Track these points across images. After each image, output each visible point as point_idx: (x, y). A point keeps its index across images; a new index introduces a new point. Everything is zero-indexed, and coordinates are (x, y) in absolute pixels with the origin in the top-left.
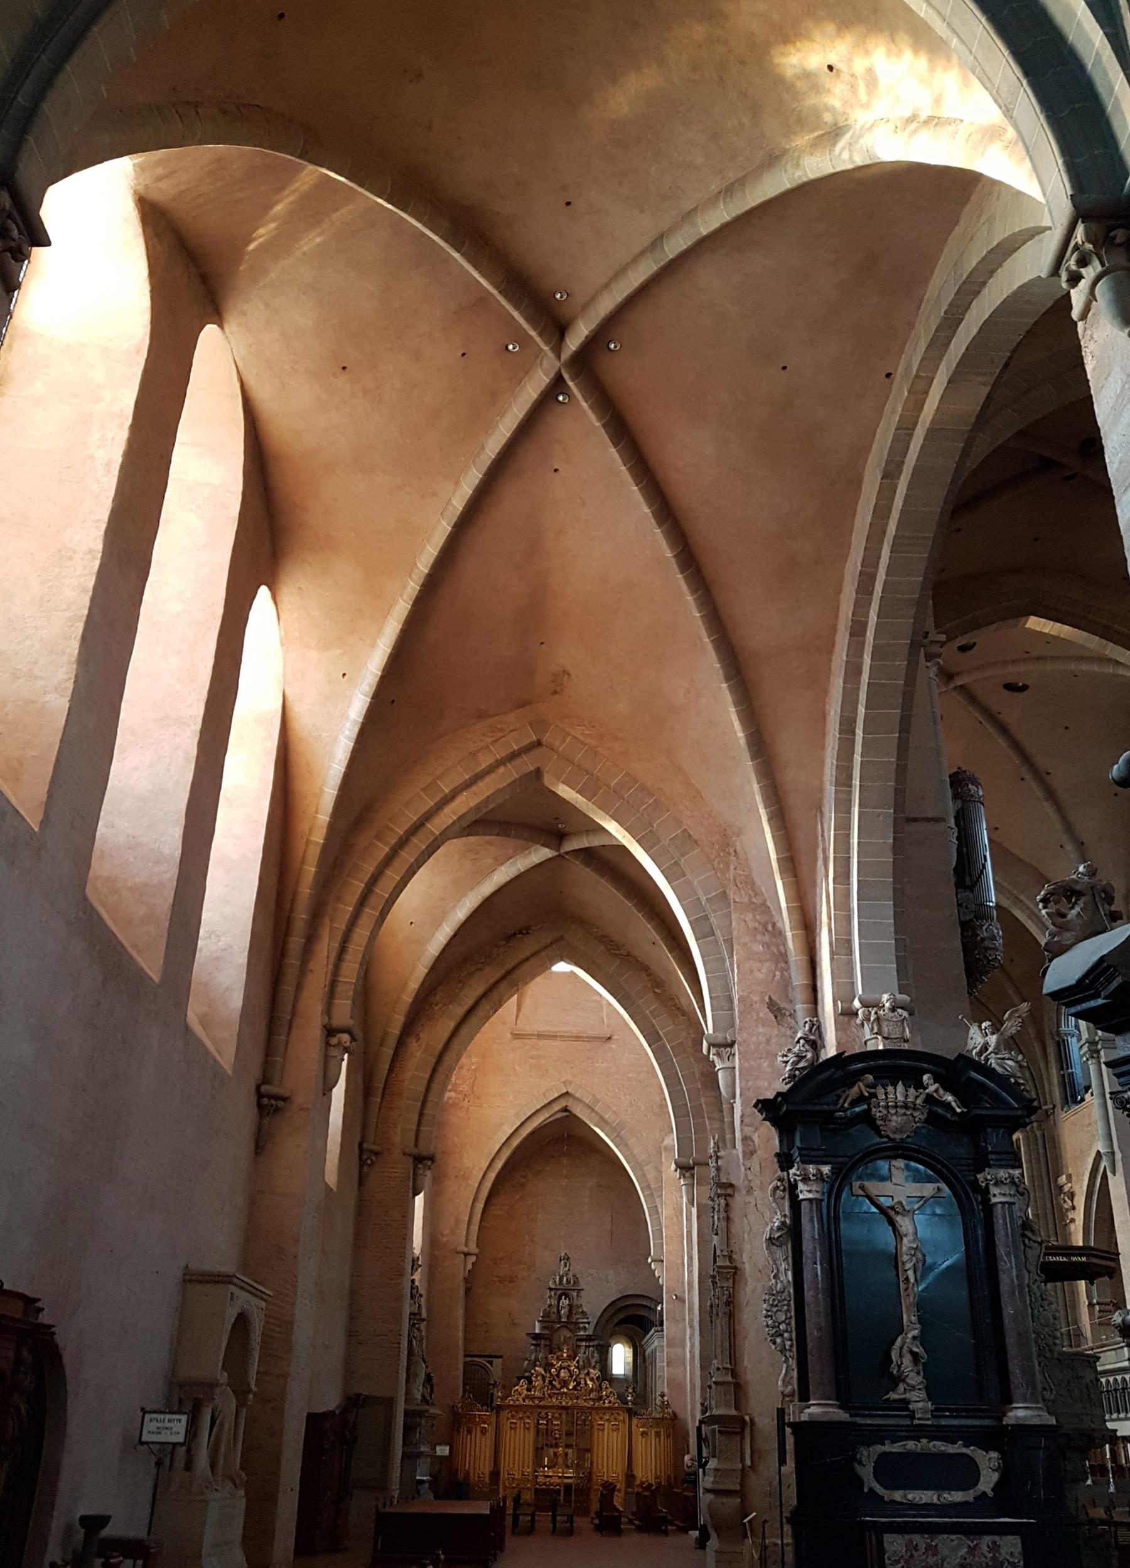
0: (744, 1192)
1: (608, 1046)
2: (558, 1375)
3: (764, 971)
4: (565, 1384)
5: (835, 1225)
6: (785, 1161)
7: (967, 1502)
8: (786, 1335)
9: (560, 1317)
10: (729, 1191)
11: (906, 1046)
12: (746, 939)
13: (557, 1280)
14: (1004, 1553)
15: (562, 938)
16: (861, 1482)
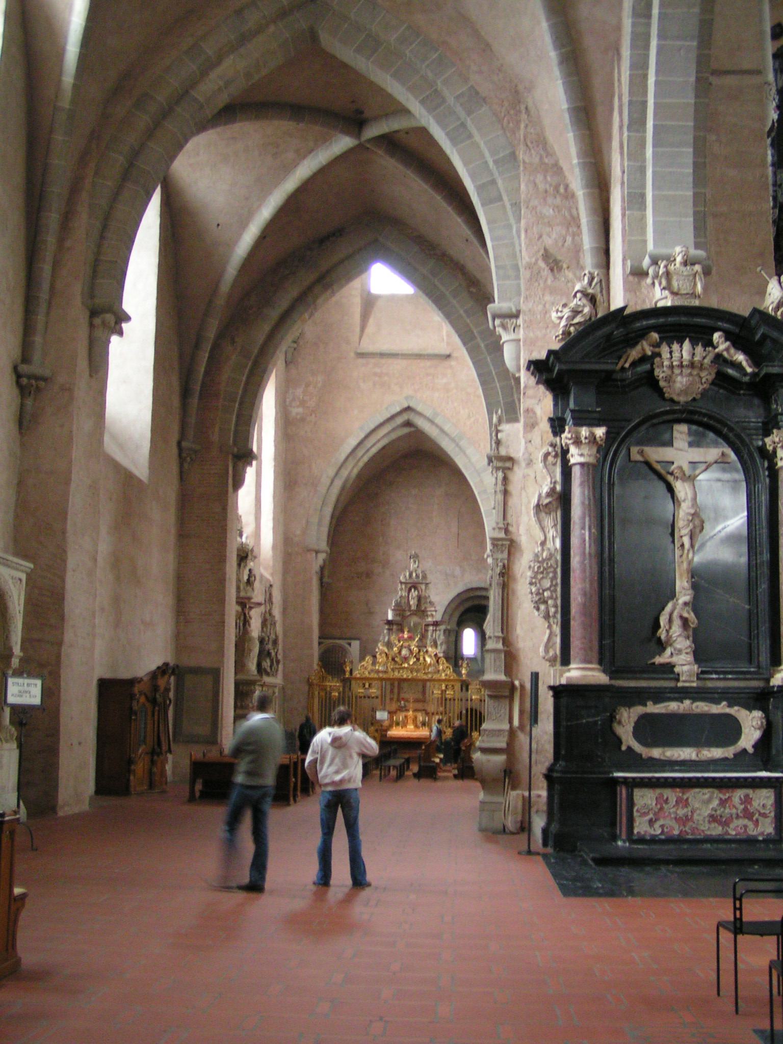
0: (523, 464)
1: (446, 363)
2: (400, 652)
3: (554, 236)
4: (406, 659)
5: (609, 490)
6: (557, 425)
7: (726, 759)
8: (550, 602)
9: (410, 606)
10: (508, 464)
11: (696, 303)
12: (535, 202)
13: (407, 574)
14: (756, 804)
15: (376, 240)
16: (619, 741)
